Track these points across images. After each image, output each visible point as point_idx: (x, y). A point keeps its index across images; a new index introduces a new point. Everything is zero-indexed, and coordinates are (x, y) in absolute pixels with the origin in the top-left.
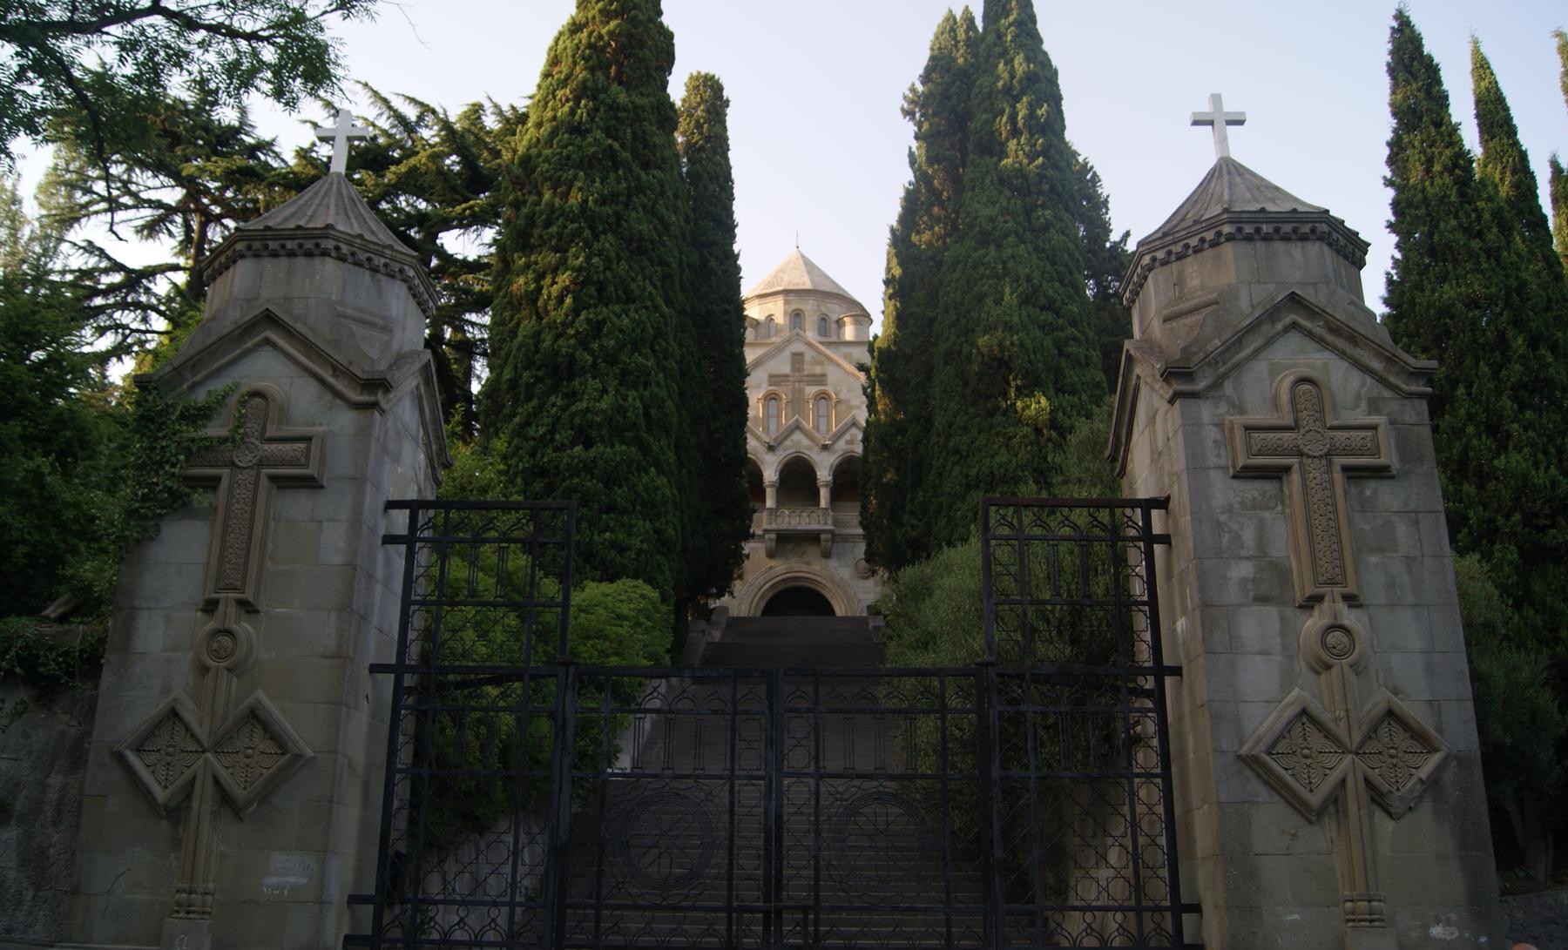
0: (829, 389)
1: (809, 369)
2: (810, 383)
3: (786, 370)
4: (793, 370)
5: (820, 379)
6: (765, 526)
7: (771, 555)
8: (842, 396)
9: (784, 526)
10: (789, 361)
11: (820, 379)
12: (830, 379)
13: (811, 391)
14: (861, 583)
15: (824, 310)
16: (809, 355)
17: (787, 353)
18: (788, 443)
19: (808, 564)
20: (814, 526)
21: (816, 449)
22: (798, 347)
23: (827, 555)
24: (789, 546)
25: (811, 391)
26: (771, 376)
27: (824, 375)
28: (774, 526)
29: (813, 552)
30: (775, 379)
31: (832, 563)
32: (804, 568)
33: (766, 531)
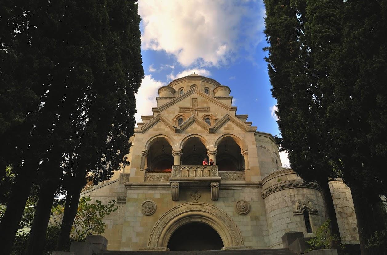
0: (211, 113)
1: (200, 105)
2: (201, 111)
3: (189, 105)
4: (192, 105)
5: (207, 109)
6: (173, 178)
7: (176, 198)
8: (218, 117)
9: (185, 178)
10: (190, 101)
11: (207, 109)
12: (211, 109)
13: (201, 114)
14: (242, 218)
15: (207, 86)
16: (200, 99)
17: (189, 98)
18: (189, 129)
19: (202, 205)
20: (206, 177)
21: (206, 132)
22: (194, 95)
23: (215, 199)
24: (189, 193)
25: (201, 114)
26: (180, 108)
28: (178, 177)
29: (206, 197)
30: (183, 109)
31: (220, 204)
32: (199, 208)
33: (172, 181)
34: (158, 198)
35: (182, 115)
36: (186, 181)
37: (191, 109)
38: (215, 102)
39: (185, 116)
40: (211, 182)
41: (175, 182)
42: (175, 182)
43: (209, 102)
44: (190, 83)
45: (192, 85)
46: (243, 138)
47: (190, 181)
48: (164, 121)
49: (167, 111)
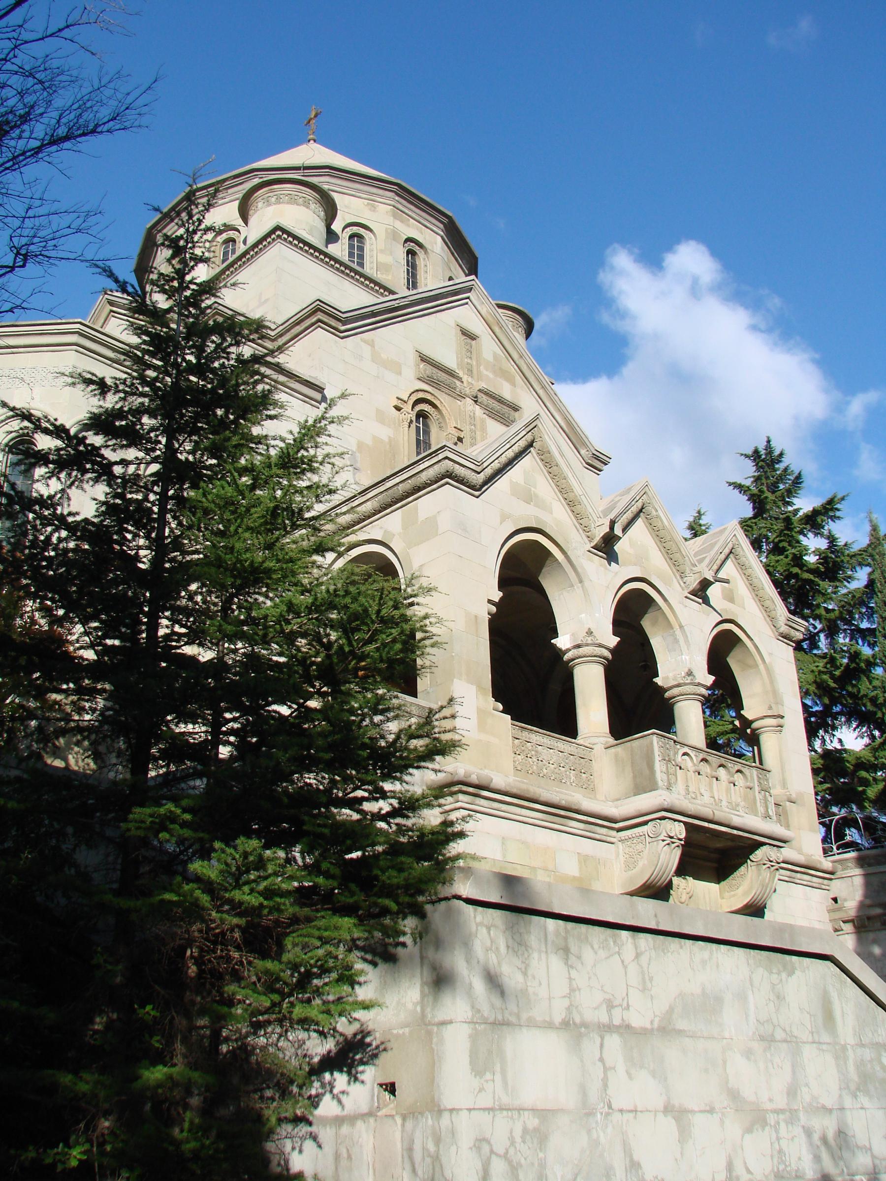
27: (516, 409)
34: (574, 877)
35: (429, 397)
36: (706, 824)
37: (458, 383)
38: (541, 392)
39: (444, 412)
40: (763, 844)
41: (675, 820)
42: (675, 820)
43: (518, 379)
44: (402, 222)
45: (409, 240)
46: (770, 654)
47: (706, 824)
48: (548, 463)
49: (372, 344)
